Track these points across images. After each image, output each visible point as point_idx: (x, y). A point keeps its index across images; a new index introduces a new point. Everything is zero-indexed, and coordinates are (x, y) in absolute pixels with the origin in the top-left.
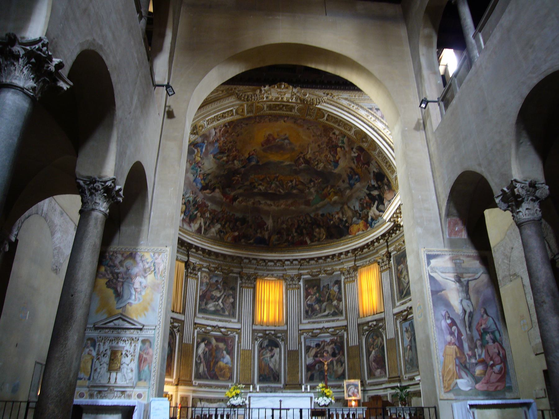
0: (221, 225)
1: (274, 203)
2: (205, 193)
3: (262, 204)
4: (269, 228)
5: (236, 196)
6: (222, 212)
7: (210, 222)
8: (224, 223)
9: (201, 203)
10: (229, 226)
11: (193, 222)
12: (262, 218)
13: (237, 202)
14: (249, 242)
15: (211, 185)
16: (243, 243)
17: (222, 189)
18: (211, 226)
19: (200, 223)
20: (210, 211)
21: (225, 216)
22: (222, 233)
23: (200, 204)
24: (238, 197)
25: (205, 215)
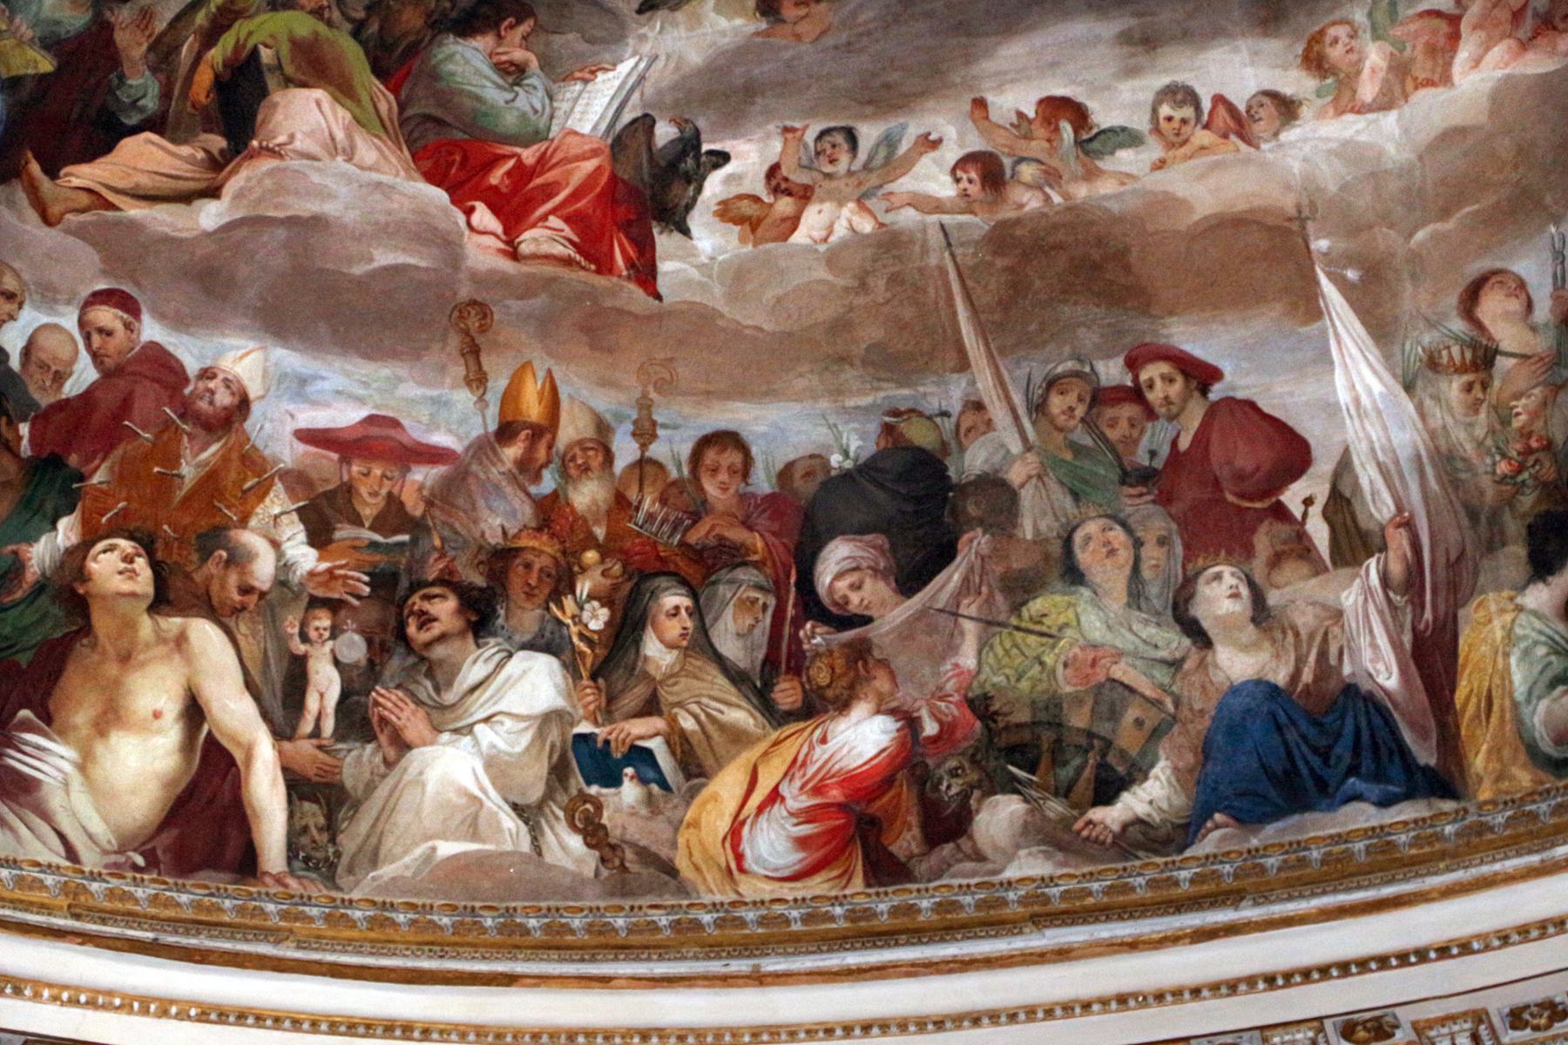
0: (571, 667)
1: (1315, 62)
2: (97, 200)
3: (1125, 137)
4: (1379, 506)
5: (665, 132)
6: (512, 452)
7: (354, 648)
8: (598, 619)
9: (84, 375)
10: (700, 644)
11: (48, 719)
12: (1201, 375)
13: (698, 220)
14: (1112, 816)
15: (163, 53)
16: (1030, 865)
17: (379, 71)
18: (388, 700)
19: (194, 711)
20: (297, 480)
21: (587, 495)
22: (614, 781)
23: (88, 396)
24: (689, 143)
25: (239, 559)
